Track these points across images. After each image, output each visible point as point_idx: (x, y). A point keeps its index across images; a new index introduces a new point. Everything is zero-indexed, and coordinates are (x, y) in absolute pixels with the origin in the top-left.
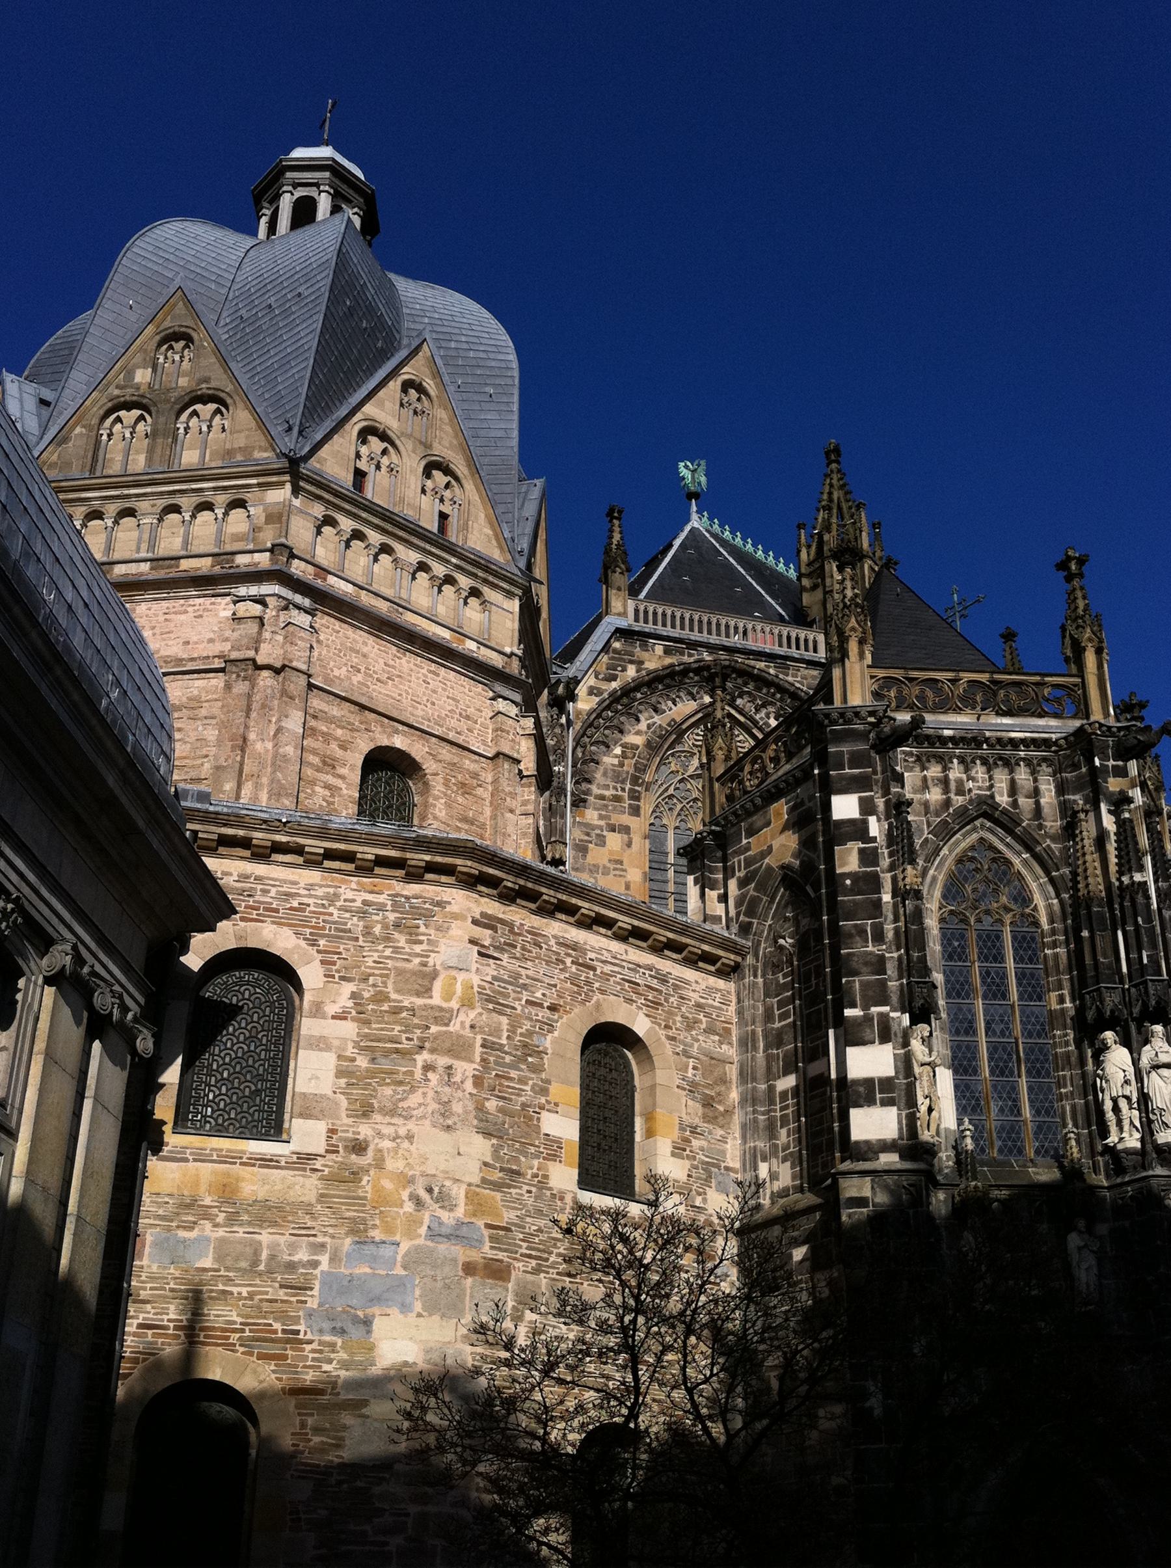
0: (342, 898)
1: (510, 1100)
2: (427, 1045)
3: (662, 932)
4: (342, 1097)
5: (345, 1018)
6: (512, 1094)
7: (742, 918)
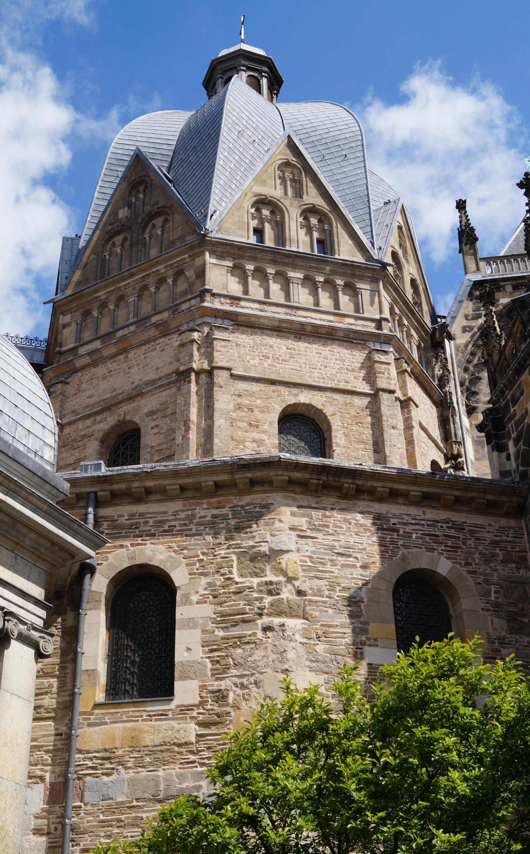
0: (197, 517)
1: (336, 642)
3: (448, 492)
4: (208, 660)
5: (206, 602)
6: (336, 638)
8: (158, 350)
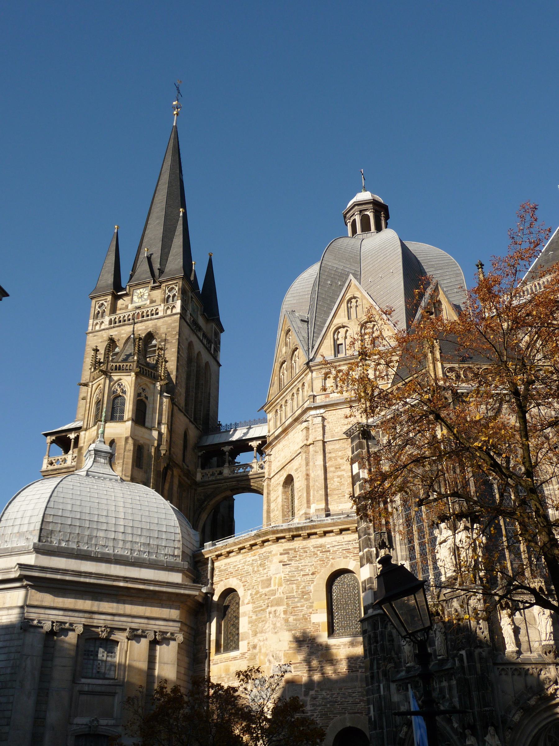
2: (270, 605)
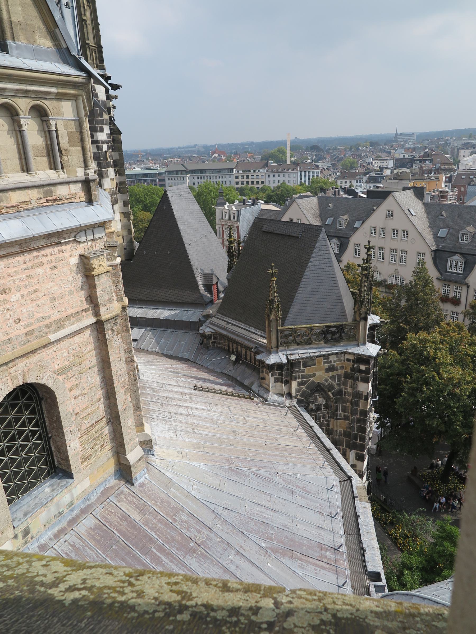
7: (298, 397)
8: (47, 267)
